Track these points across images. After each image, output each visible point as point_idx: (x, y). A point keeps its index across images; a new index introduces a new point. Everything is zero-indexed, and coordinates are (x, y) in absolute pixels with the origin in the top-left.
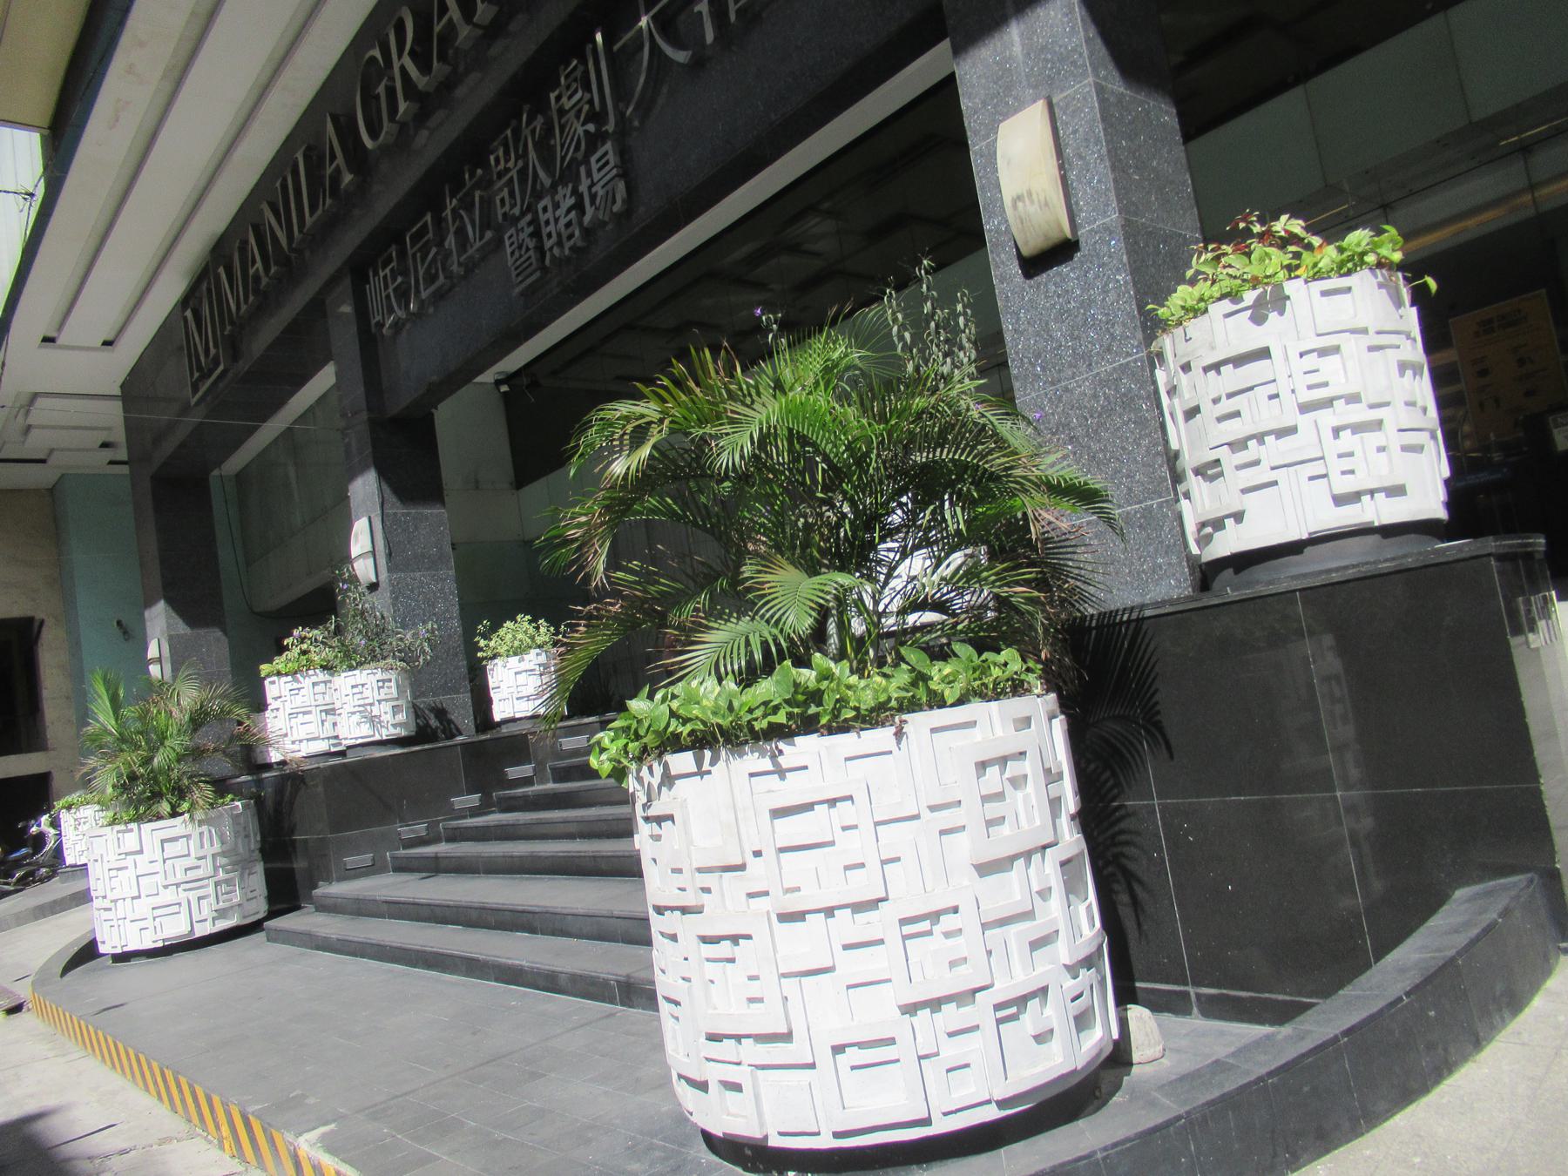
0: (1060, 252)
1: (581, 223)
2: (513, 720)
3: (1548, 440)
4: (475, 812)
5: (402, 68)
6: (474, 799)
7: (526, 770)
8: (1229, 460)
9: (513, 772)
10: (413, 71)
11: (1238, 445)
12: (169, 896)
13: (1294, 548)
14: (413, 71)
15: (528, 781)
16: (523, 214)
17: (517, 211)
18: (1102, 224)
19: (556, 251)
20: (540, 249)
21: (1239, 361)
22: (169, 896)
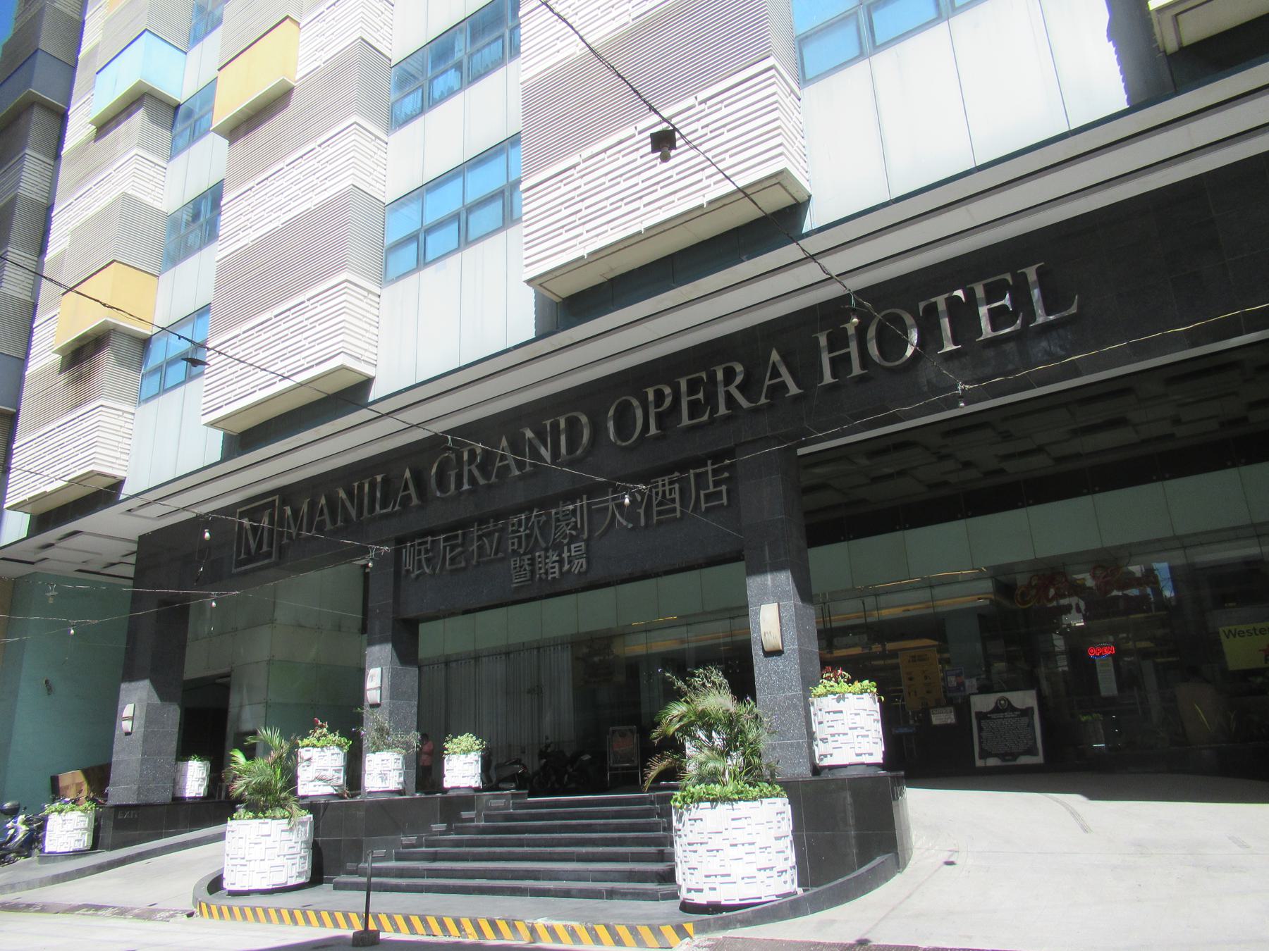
0: (777, 653)
1: (561, 568)
2: (458, 788)
3: (929, 720)
4: (442, 833)
5: (470, 471)
6: (443, 827)
7: (472, 814)
8: (830, 739)
9: (465, 815)
10: (476, 473)
11: (833, 735)
12: (279, 861)
13: (845, 766)
14: (476, 473)
15: (472, 820)
16: (525, 554)
17: (522, 551)
18: (792, 647)
19: (544, 576)
20: (533, 572)
21: (835, 712)
22: (279, 861)
